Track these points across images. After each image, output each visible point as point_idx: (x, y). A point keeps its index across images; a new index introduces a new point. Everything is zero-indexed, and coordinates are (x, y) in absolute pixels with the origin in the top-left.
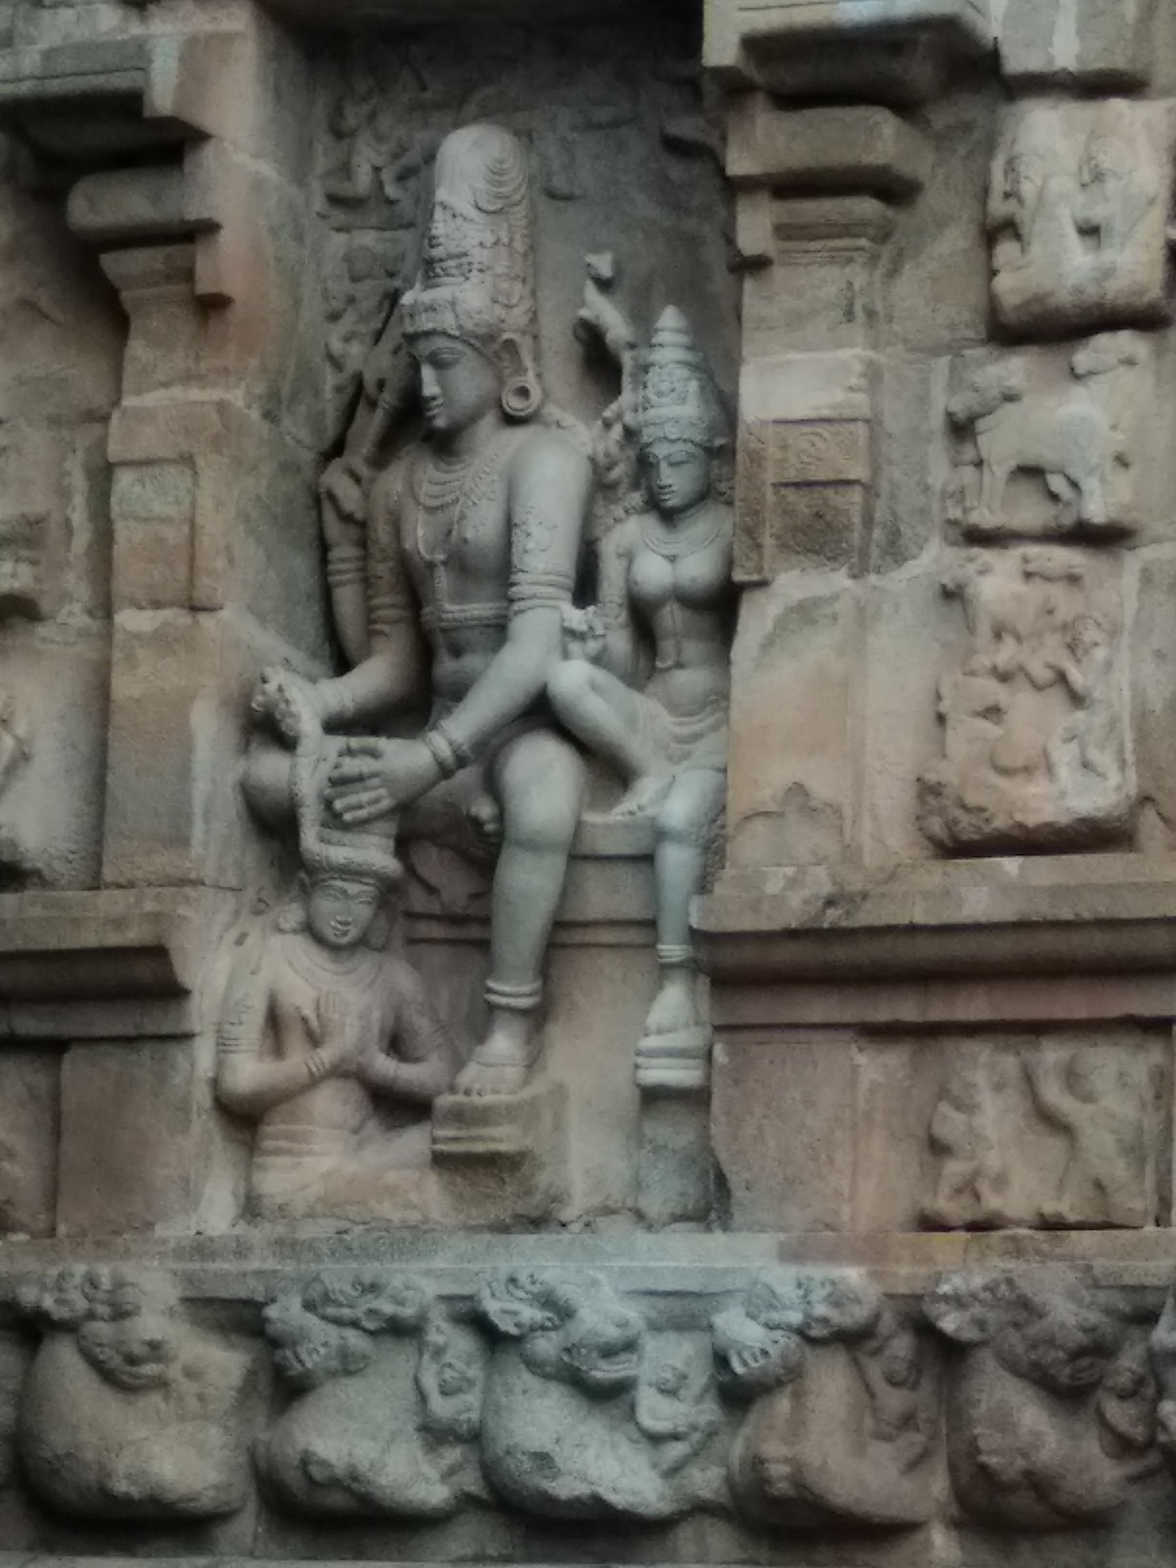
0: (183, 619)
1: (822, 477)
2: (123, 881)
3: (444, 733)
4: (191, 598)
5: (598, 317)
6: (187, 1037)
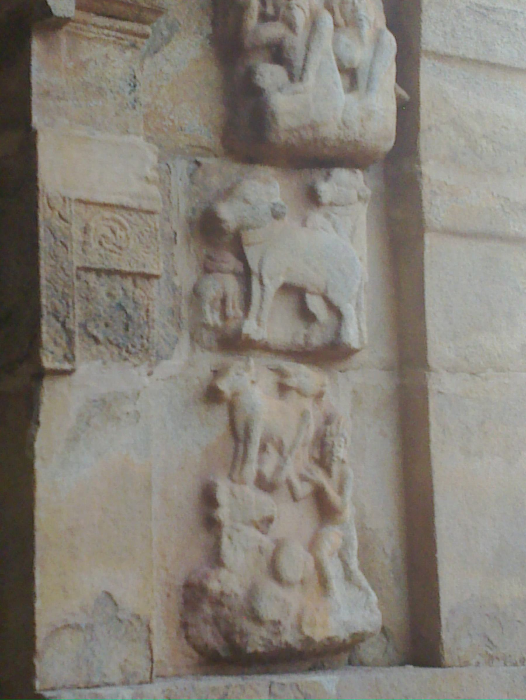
1: (126, 268)
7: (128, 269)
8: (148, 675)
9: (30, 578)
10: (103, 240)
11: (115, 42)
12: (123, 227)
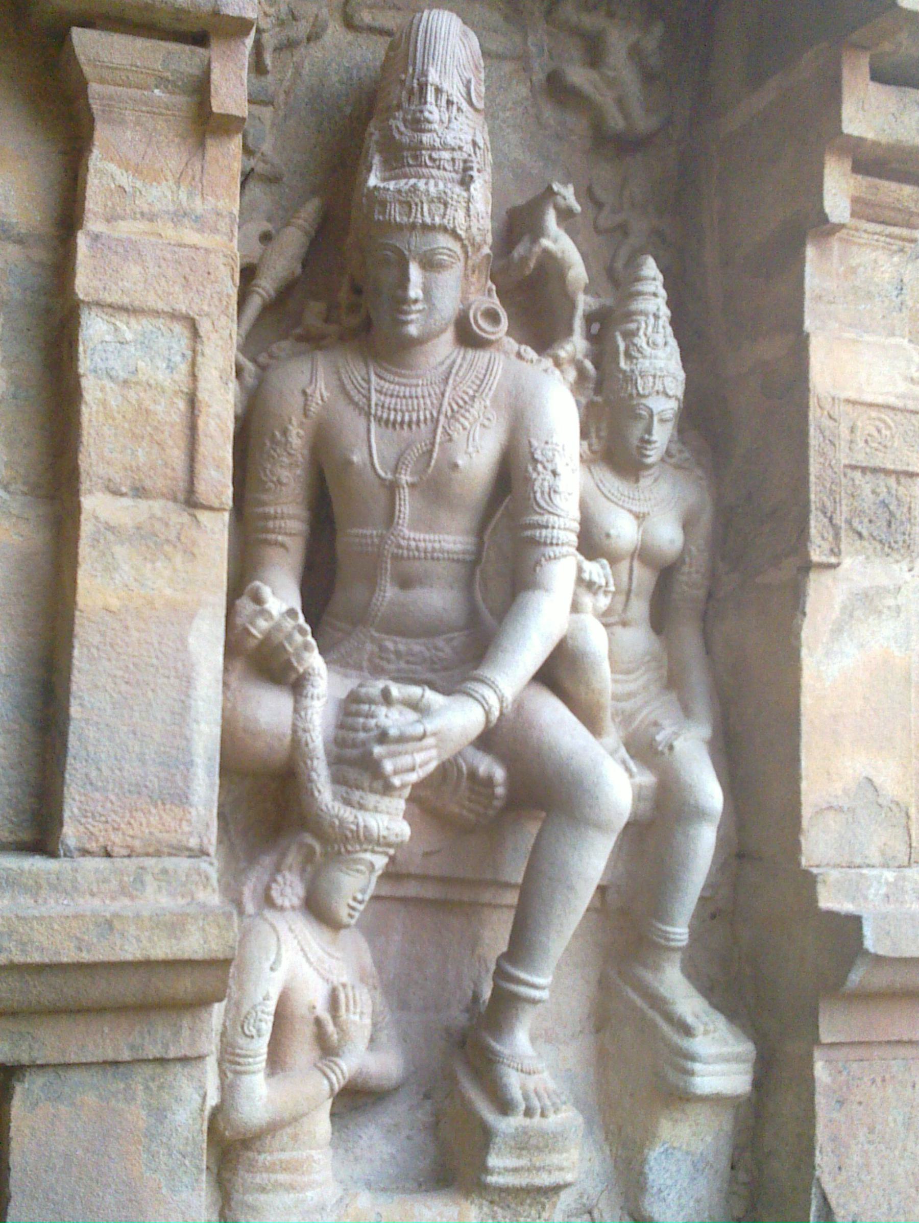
0: (178, 517)
1: (890, 466)
2: (93, 846)
3: (492, 685)
4: (191, 490)
5: (563, 252)
6: (200, 1058)
7: (892, 467)
8: (906, 858)
9: (795, 760)
10: (869, 439)
11: (883, 248)
12: (888, 427)
